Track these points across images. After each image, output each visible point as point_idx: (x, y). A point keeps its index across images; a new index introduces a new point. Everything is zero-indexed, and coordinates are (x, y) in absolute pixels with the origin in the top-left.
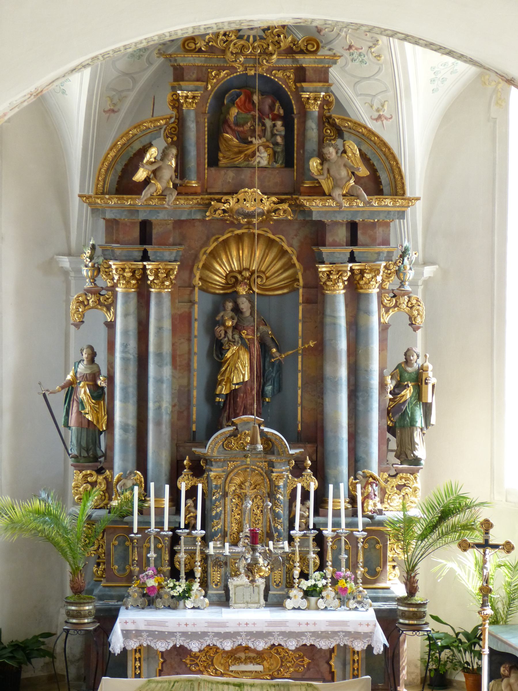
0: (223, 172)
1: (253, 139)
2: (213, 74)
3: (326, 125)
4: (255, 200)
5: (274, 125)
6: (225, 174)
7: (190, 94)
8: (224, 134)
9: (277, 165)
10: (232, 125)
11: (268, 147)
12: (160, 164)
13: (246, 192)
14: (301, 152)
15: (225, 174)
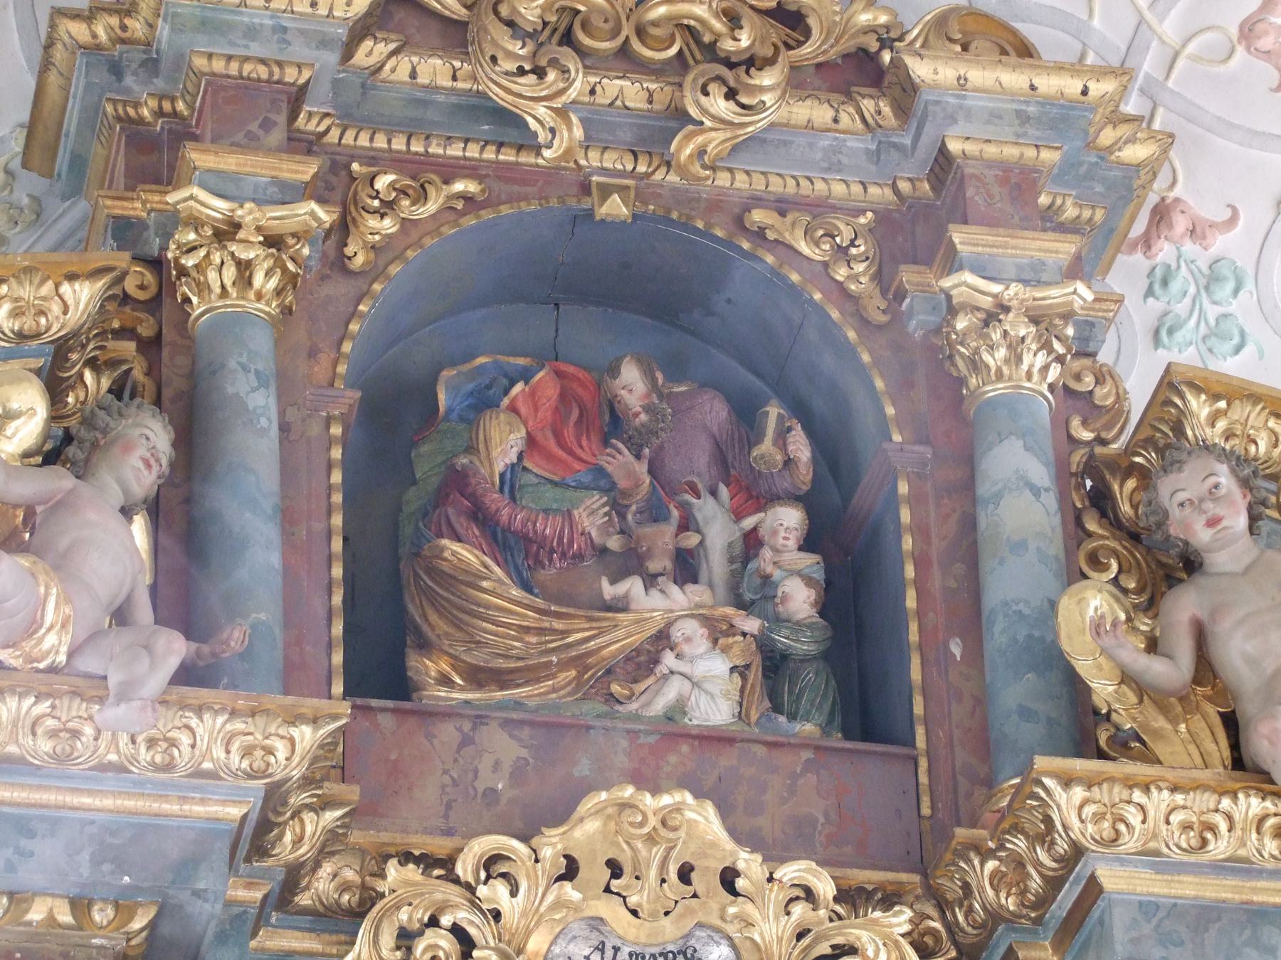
0: (448, 732)
1: (633, 586)
2: (382, 182)
3: (1092, 525)
4: (685, 875)
5: (752, 542)
6: (466, 741)
7: (248, 214)
8: (445, 542)
9: (808, 728)
10: (495, 501)
11: (732, 630)
12: (59, 480)
13: (624, 806)
14: (956, 649)
15: (466, 741)
